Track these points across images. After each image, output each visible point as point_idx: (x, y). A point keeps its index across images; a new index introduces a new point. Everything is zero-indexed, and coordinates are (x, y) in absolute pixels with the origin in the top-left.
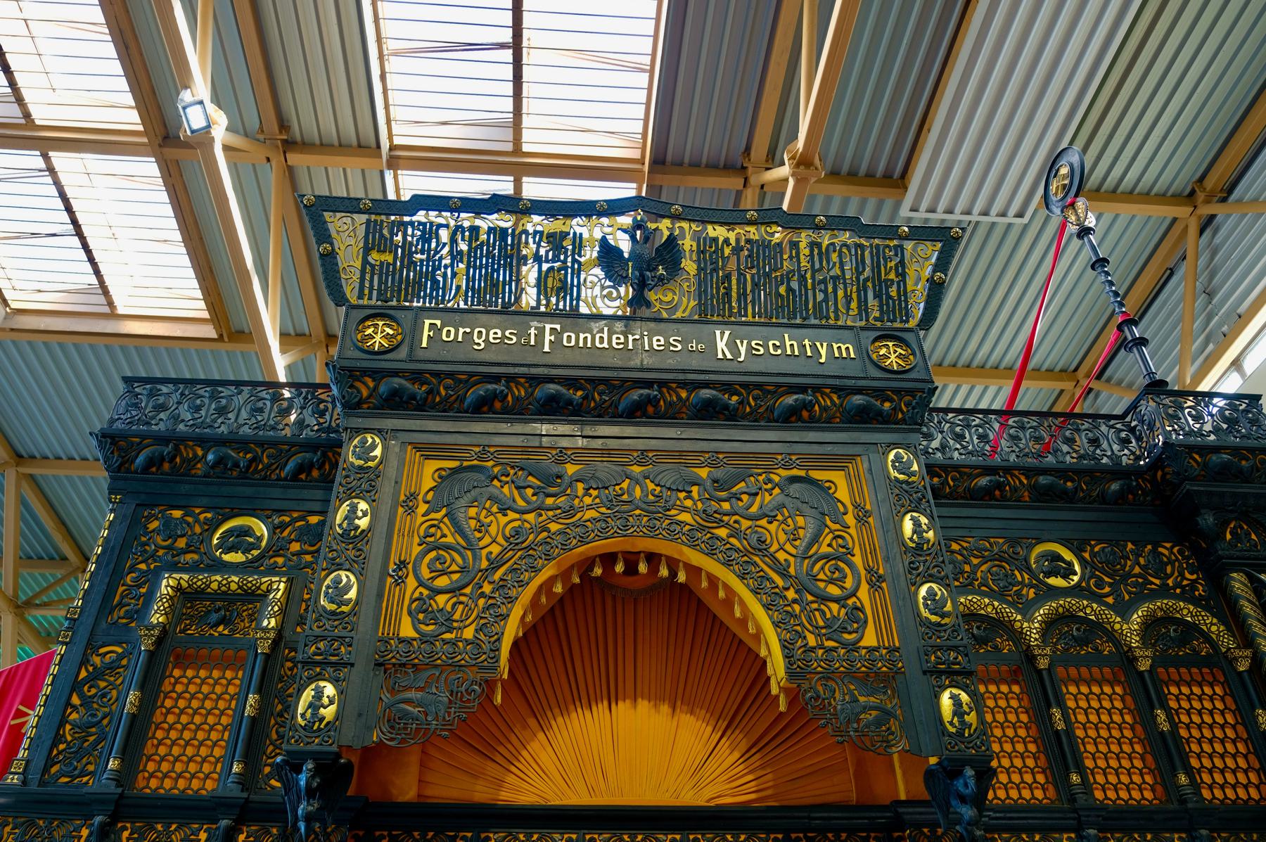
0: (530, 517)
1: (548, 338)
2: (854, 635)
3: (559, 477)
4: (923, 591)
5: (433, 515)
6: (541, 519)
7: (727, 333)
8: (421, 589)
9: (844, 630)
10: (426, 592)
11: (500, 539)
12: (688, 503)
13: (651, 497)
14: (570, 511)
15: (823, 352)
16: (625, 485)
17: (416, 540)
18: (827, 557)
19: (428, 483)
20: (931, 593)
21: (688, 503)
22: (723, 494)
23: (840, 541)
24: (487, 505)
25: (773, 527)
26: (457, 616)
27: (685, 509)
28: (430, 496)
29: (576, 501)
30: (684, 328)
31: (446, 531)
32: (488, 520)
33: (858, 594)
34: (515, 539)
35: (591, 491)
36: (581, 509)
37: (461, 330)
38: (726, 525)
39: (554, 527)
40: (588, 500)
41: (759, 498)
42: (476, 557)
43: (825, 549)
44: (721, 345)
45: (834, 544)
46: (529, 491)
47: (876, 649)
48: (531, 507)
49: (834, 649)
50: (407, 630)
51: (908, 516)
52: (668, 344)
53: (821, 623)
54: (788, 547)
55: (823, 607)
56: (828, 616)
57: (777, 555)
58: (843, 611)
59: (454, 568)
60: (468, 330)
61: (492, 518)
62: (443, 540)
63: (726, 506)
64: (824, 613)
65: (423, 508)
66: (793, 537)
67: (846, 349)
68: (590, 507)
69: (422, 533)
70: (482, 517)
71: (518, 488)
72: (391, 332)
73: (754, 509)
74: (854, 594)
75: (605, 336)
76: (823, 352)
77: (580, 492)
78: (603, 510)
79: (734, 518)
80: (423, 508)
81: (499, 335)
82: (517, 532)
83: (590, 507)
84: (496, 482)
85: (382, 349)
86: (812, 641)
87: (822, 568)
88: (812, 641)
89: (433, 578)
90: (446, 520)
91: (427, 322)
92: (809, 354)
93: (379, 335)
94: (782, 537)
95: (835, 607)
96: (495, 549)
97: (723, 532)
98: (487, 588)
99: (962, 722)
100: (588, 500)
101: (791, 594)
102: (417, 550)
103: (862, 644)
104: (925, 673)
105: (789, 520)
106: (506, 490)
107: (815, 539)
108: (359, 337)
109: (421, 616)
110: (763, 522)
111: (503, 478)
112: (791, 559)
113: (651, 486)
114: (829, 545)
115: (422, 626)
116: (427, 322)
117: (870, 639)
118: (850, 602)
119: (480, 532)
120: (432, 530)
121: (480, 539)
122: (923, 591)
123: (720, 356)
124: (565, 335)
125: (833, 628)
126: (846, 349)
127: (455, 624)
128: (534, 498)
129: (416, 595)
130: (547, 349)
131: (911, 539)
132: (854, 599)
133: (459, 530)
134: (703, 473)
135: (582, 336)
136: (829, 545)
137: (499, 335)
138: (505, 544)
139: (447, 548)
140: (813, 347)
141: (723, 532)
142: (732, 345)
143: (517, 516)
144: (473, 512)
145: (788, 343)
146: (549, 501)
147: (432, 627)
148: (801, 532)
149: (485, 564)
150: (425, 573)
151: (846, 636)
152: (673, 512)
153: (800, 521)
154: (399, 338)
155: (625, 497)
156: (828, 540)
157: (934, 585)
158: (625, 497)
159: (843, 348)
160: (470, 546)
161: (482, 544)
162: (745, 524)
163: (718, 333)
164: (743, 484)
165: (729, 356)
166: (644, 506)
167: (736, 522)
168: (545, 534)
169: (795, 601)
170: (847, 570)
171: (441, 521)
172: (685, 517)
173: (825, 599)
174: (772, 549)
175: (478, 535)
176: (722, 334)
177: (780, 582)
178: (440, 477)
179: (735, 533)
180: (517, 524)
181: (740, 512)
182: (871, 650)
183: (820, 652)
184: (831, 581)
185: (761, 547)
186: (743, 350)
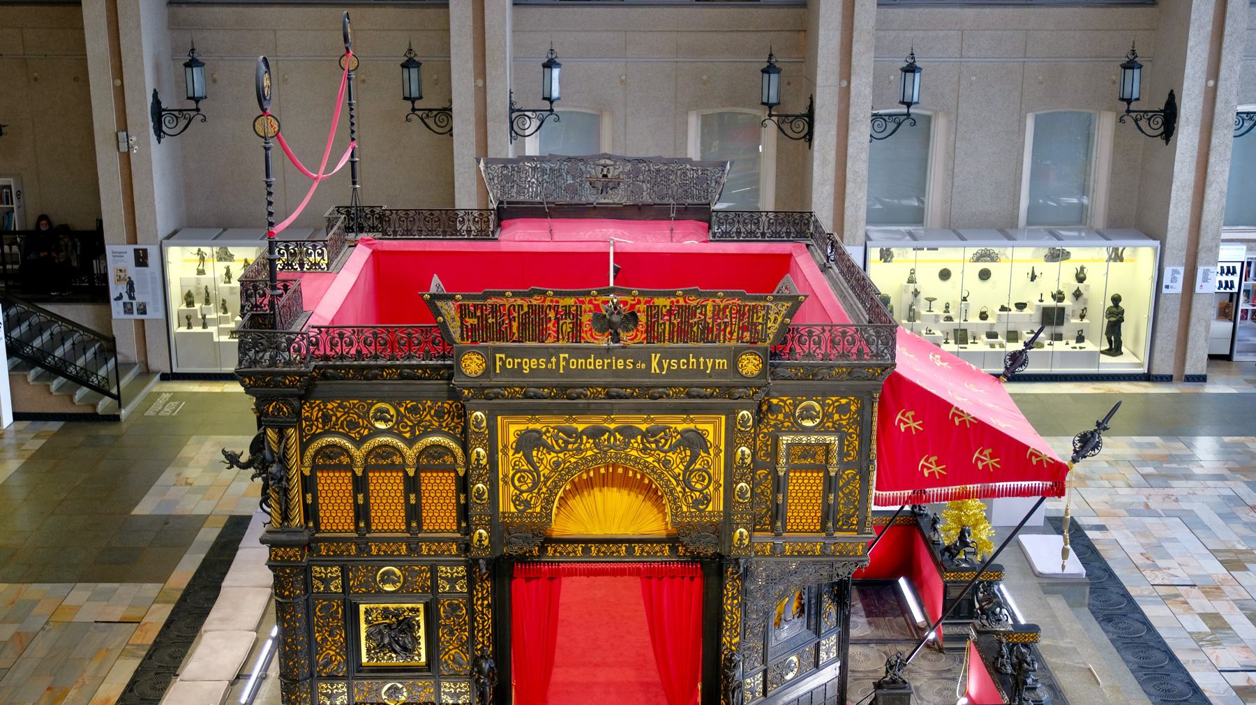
0: (561, 455)
1: (562, 363)
15: (710, 366)
18: (699, 470)
19: (512, 439)
36: (587, 450)
39: (573, 460)
42: (539, 476)
43: (698, 466)
44: (654, 364)
50: (513, 509)
52: (625, 364)
65: (511, 452)
76: (710, 366)
82: (557, 464)
83: (591, 449)
86: (685, 509)
88: (685, 509)
96: (546, 472)
97: (650, 460)
98: (544, 490)
101: (679, 489)
102: (512, 472)
113: (618, 436)
117: (710, 508)
125: (696, 503)
133: (530, 461)
139: (524, 471)
140: (705, 363)
141: (650, 460)
142: (660, 364)
160: (536, 469)
162: (662, 455)
172: (634, 453)
173: (693, 490)
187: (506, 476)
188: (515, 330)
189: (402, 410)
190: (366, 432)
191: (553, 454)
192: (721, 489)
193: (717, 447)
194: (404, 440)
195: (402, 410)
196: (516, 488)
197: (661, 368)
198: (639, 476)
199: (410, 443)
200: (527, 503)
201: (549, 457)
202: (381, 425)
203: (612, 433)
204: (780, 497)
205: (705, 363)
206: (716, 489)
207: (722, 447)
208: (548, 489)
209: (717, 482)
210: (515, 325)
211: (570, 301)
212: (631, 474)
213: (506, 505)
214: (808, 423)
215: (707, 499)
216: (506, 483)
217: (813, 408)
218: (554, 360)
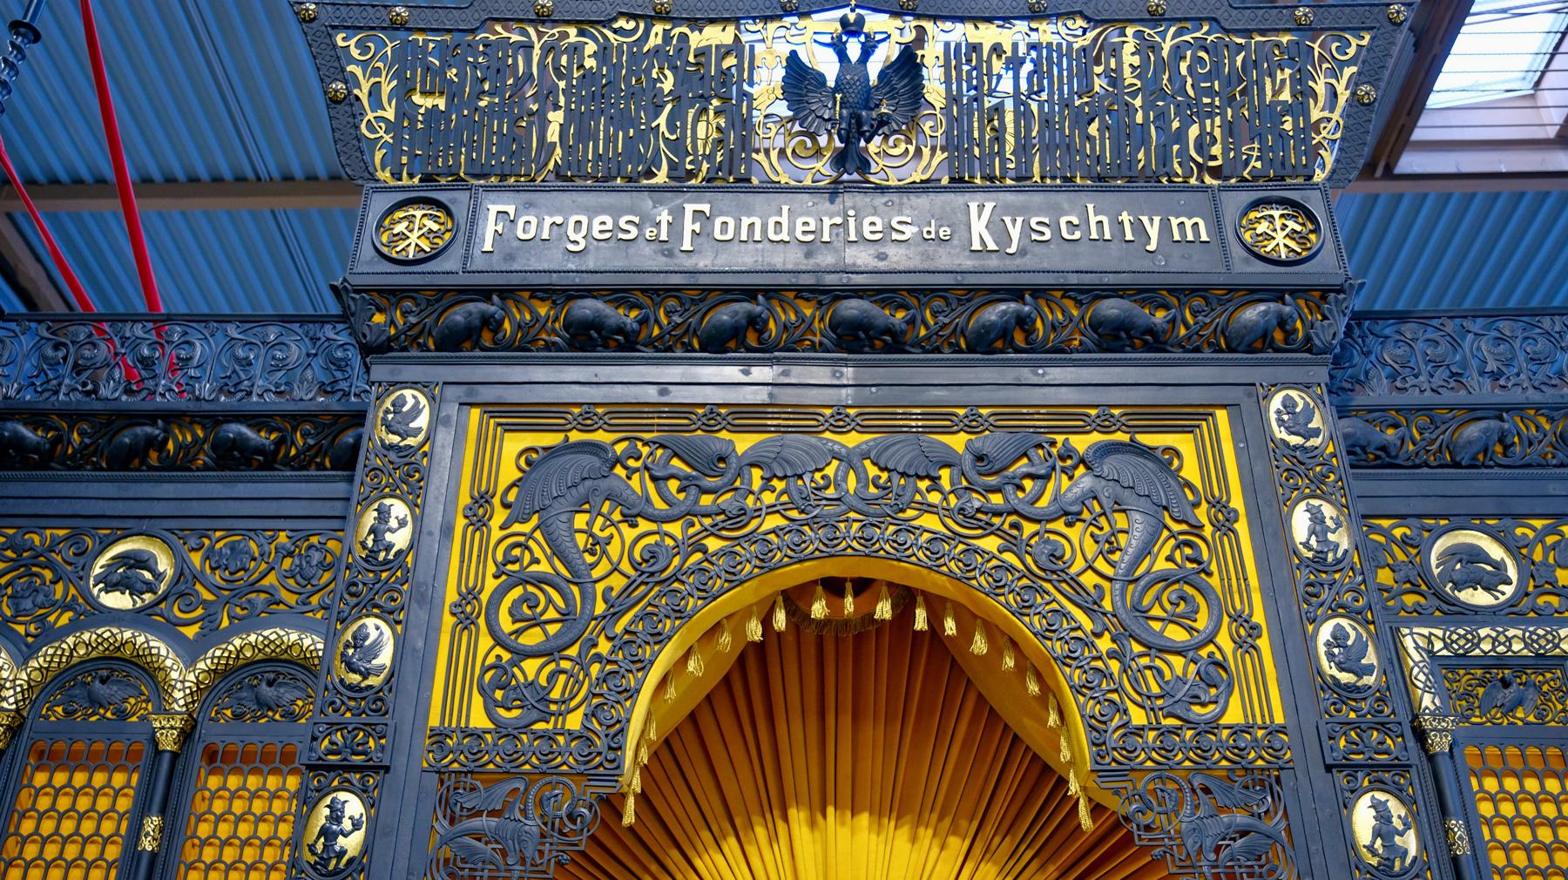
0: (675, 528)
1: (689, 226)
2: (1212, 707)
3: (722, 459)
4: (1325, 632)
5: (517, 527)
6: (691, 531)
7: (989, 206)
8: (498, 651)
9: (1196, 699)
10: (506, 656)
11: (625, 566)
12: (934, 498)
13: (872, 490)
14: (739, 517)
15: (1154, 232)
16: (830, 471)
17: (491, 569)
18: (1165, 579)
20: (1339, 637)
21: (934, 498)
22: (992, 480)
23: (1188, 551)
24: (605, 509)
25: (1074, 533)
26: (555, 694)
27: (930, 508)
28: (511, 497)
29: (750, 500)
30: (923, 201)
31: (538, 553)
32: (606, 533)
33: (1218, 640)
34: (649, 568)
35: (775, 482)
37: (548, 220)
38: (997, 532)
39: (713, 544)
40: (768, 498)
41: (1051, 486)
42: (589, 598)
43: (1161, 565)
44: (979, 227)
45: (1177, 555)
46: (673, 485)
47: (1248, 728)
48: (676, 511)
49: (1174, 731)
50: (479, 719)
51: (1302, 506)
53: (1155, 689)
54: (1100, 564)
55: (1158, 663)
56: (1168, 675)
57: (1082, 579)
58: (1192, 668)
59: (551, 614)
60: (559, 220)
61: (612, 530)
62: (534, 568)
63: (996, 499)
64: (1160, 672)
65: (500, 516)
66: (1109, 547)
67: (1193, 226)
68: (772, 510)
69: (500, 558)
70: (596, 530)
71: (654, 479)
72: (435, 227)
73: (1043, 502)
74: (1211, 641)
75: (784, 220)
76: (1154, 232)
77: (757, 484)
78: (794, 514)
79: (1013, 518)
80: (500, 516)
81: (609, 226)
82: (652, 555)
83: (772, 510)
84: (619, 470)
85: (422, 255)
87: (1158, 598)
88: (1138, 717)
89: (518, 632)
90: (538, 535)
91: (494, 209)
92: (1129, 236)
93: (417, 233)
94: (1091, 548)
95: (1178, 662)
96: (617, 582)
98: (604, 647)
99: (1389, 846)
100: (768, 498)
101: (1104, 644)
102: (491, 584)
103: (1224, 721)
104: (1329, 768)
105: (1103, 520)
106: (635, 482)
107: (1146, 550)
108: (384, 239)
109: (499, 694)
110: (1059, 525)
111: (631, 463)
112: (1106, 585)
113: (873, 471)
114: (1170, 559)
115: (501, 711)
116: (494, 209)
118: (1204, 653)
119: (593, 554)
120: (517, 552)
121: (593, 566)
122: (1325, 632)
123: (976, 246)
124: (718, 221)
125: (1172, 698)
126: (1193, 226)
127: (553, 707)
128: (682, 496)
129: (491, 660)
130: (687, 246)
131: (1306, 545)
132: (1211, 648)
133: (558, 551)
134: (958, 442)
135: (746, 221)
136: (1170, 559)
137: (609, 226)
138: (631, 572)
139: (540, 581)
141: (991, 544)
142: (997, 228)
143: (653, 527)
144: (580, 521)
145: (1093, 220)
146: (706, 500)
147: (516, 713)
148: (1122, 538)
149: (600, 607)
150: (506, 624)
151: (1197, 709)
152: (910, 513)
153: (1121, 521)
154: (447, 236)
155: (831, 492)
156: (1166, 551)
157: (1344, 622)
158: (831, 492)
159: (1189, 223)
160: (580, 578)
161: (596, 574)
162: (1029, 528)
163: (973, 206)
164: (1025, 461)
165: (992, 246)
166: (861, 505)
167: (1014, 526)
168: (698, 556)
169: (1112, 655)
170: (1199, 599)
171: (530, 536)
174: (1073, 570)
175: (589, 559)
176: (981, 207)
177: (1088, 625)
178: (528, 463)
179: (1012, 544)
180: (651, 540)
181: (1020, 508)
182: (1236, 730)
183: (1152, 735)
184: (1172, 620)
185: (1055, 566)
186: (1015, 233)
187: (469, 595)
188: (553, 134)
189: (196, 558)
190: (65, 619)
191: (644, 526)
192: (1263, 643)
193: (1220, 505)
194: (176, 641)
195: (196, 558)
196: (499, 641)
197: (1003, 237)
198: (950, 626)
199: (190, 653)
200: (538, 701)
201: (629, 534)
202: (117, 600)
203: (849, 460)
204: (1457, 827)
205: (1139, 228)
206: (1246, 644)
207: (1237, 502)
208: (620, 644)
209: (1240, 619)
210: (556, 117)
211: (716, 36)
212: (921, 621)
213: (456, 703)
214: (1478, 597)
215: (1215, 676)
216: (466, 621)
217: (1477, 555)
218: (664, 217)
